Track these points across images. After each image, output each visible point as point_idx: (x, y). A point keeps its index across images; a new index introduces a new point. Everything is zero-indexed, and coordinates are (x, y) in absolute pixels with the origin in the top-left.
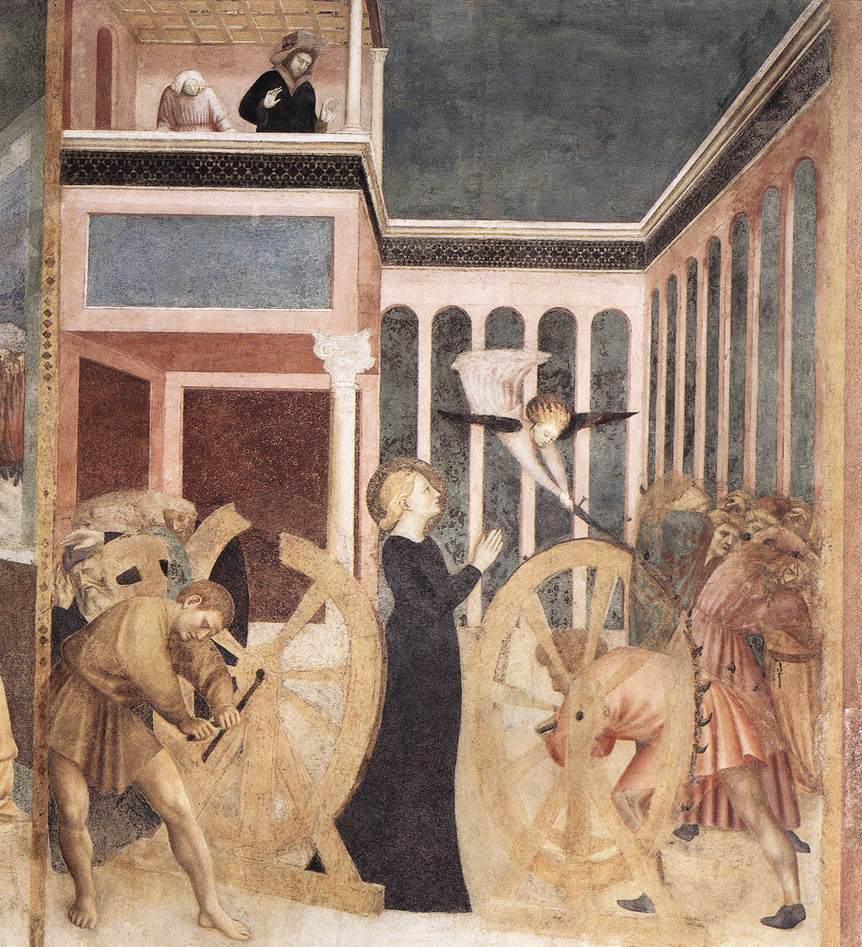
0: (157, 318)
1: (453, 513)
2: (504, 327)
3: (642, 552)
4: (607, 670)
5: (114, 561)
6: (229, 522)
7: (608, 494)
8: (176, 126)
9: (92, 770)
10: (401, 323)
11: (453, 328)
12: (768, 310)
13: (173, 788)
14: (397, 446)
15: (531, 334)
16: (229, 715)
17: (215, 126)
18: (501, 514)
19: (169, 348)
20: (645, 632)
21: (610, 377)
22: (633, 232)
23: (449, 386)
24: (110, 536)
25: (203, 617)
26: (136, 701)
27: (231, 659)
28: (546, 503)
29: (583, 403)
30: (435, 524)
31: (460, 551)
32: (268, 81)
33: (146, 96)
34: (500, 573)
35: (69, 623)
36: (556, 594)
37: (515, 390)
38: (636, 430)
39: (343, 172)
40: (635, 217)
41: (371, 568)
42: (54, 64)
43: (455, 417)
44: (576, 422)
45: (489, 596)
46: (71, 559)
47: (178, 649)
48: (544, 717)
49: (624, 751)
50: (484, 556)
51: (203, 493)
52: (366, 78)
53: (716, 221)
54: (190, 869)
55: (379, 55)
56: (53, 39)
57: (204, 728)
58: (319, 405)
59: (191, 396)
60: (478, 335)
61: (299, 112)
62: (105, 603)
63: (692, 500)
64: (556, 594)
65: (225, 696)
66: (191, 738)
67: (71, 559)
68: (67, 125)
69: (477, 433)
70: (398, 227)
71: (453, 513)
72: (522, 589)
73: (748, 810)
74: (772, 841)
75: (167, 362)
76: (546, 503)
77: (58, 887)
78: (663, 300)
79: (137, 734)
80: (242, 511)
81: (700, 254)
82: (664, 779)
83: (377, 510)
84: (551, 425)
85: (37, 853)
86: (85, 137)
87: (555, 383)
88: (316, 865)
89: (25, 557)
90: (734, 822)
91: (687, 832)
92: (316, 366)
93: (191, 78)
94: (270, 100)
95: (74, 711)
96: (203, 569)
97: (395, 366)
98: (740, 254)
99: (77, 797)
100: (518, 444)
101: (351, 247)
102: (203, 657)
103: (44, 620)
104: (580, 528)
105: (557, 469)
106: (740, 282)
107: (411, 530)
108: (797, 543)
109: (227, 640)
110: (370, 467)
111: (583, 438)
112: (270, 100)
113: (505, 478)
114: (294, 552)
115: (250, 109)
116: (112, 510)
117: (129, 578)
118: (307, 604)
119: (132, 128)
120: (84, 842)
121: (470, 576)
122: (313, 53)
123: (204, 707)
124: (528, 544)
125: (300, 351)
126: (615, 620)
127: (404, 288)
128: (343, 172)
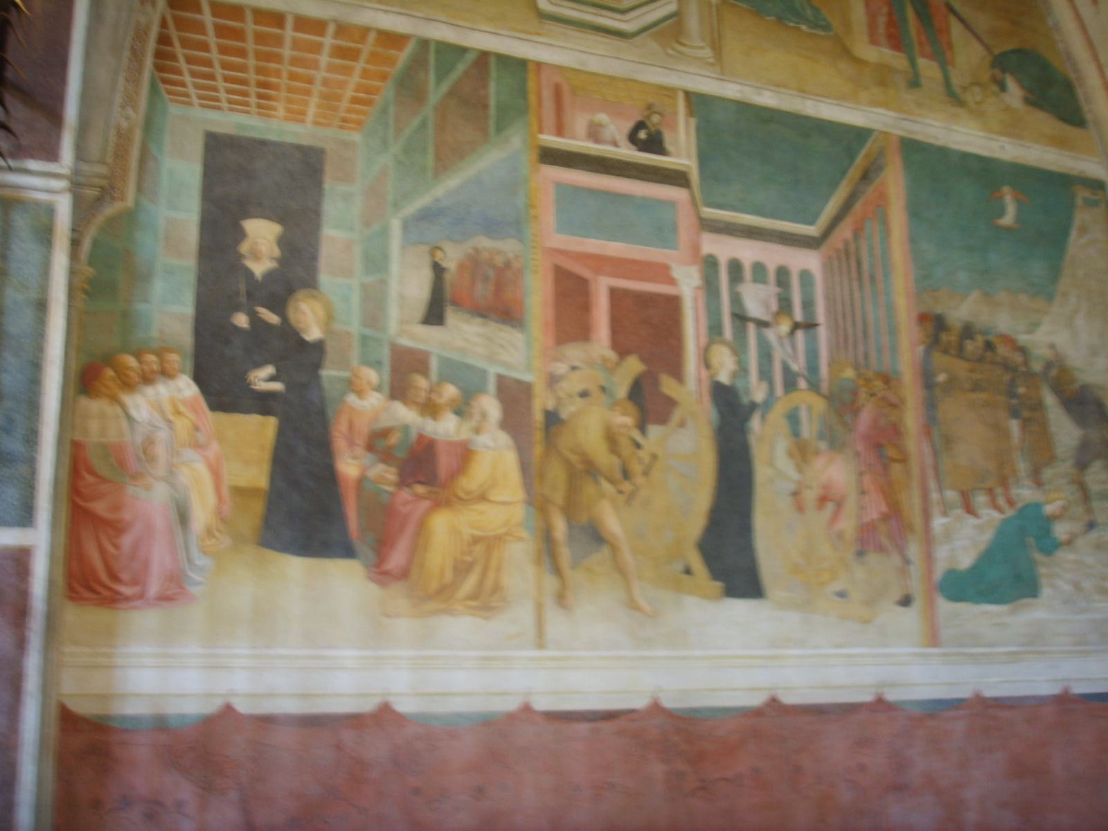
0: (594, 245)
1: (742, 370)
2: (759, 270)
3: (830, 398)
4: (819, 463)
5: (574, 384)
6: (634, 366)
7: (813, 368)
8: (597, 140)
9: (569, 510)
10: (710, 264)
11: (735, 268)
12: (873, 279)
13: (612, 523)
14: (715, 330)
15: (772, 276)
16: (640, 480)
17: (615, 144)
18: (766, 375)
19: (602, 263)
20: (836, 445)
21: (808, 305)
22: (812, 230)
23: (736, 299)
24: (574, 368)
25: (624, 420)
26: (590, 469)
27: (638, 446)
28: (786, 369)
29: (798, 316)
30: (734, 375)
31: (748, 391)
32: (640, 125)
33: (580, 123)
34: (767, 405)
35: (552, 419)
36: (793, 418)
37: (766, 305)
38: (823, 333)
39: (677, 178)
40: (811, 223)
41: (707, 399)
42: (532, 98)
43: (741, 318)
44: (796, 326)
45: (763, 417)
46: (553, 381)
47: (612, 439)
48: (792, 487)
49: (830, 507)
50: (759, 395)
51: (621, 349)
52: (687, 134)
53: (845, 231)
54: (621, 570)
55: (693, 121)
56: (531, 85)
57: (627, 487)
58: (673, 303)
59: (614, 293)
60: (748, 274)
61: (654, 144)
62: (572, 409)
63: (849, 373)
64: (793, 418)
65: (636, 468)
66: (621, 492)
67: (553, 381)
68: (541, 131)
69: (751, 328)
70: (709, 212)
71: (742, 370)
72: (777, 414)
73: (885, 542)
74: (896, 559)
75: (598, 271)
76: (786, 369)
77: (550, 583)
78: (827, 267)
79: (589, 489)
80: (643, 359)
81: (840, 246)
82: (848, 524)
83: (708, 366)
84: (785, 327)
85: (538, 562)
86: (550, 139)
87: (785, 306)
88: (688, 571)
89: (527, 377)
90: (881, 549)
91: (860, 554)
92: (672, 282)
93: (602, 117)
94: (642, 135)
95: (557, 473)
96: (622, 391)
97: (710, 285)
98: (857, 249)
99: (560, 527)
100: (770, 334)
101: (686, 222)
102: (624, 442)
103: (538, 417)
104: (802, 384)
105: (789, 350)
106: (859, 263)
107: (724, 378)
108: (894, 400)
109: (636, 435)
110: (703, 340)
111: (800, 335)
112: (642, 135)
113: (766, 355)
114: (668, 386)
115: (633, 138)
116: (574, 352)
117: (584, 394)
118: (676, 416)
119: (574, 138)
120: (565, 554)
121: (753, 406)
122: (660, 114)
123: (626, 474)
124: (779, 390)
125: (662, 272)
126: (821, 437)
127: (714, 245)
128: (677, 178)
